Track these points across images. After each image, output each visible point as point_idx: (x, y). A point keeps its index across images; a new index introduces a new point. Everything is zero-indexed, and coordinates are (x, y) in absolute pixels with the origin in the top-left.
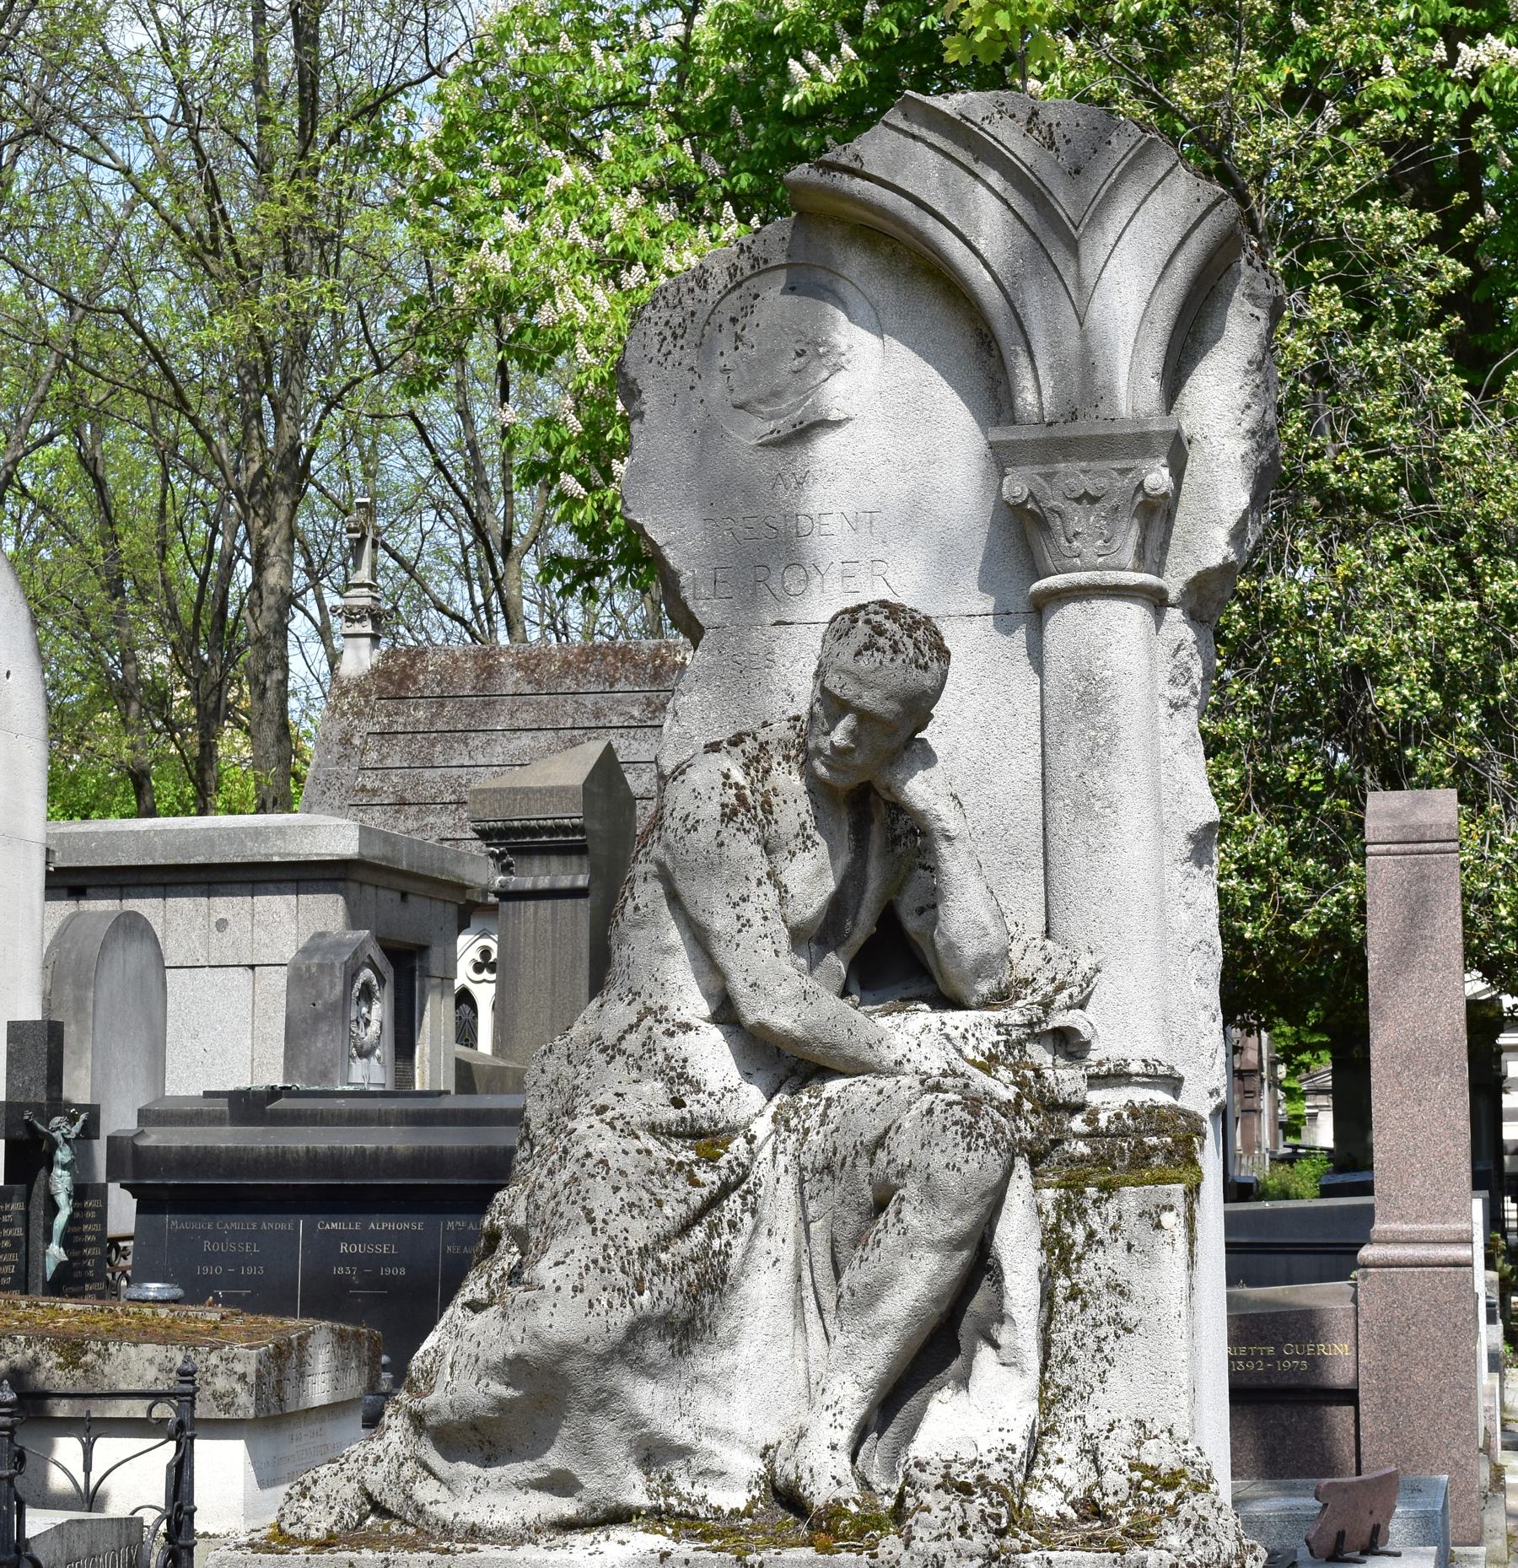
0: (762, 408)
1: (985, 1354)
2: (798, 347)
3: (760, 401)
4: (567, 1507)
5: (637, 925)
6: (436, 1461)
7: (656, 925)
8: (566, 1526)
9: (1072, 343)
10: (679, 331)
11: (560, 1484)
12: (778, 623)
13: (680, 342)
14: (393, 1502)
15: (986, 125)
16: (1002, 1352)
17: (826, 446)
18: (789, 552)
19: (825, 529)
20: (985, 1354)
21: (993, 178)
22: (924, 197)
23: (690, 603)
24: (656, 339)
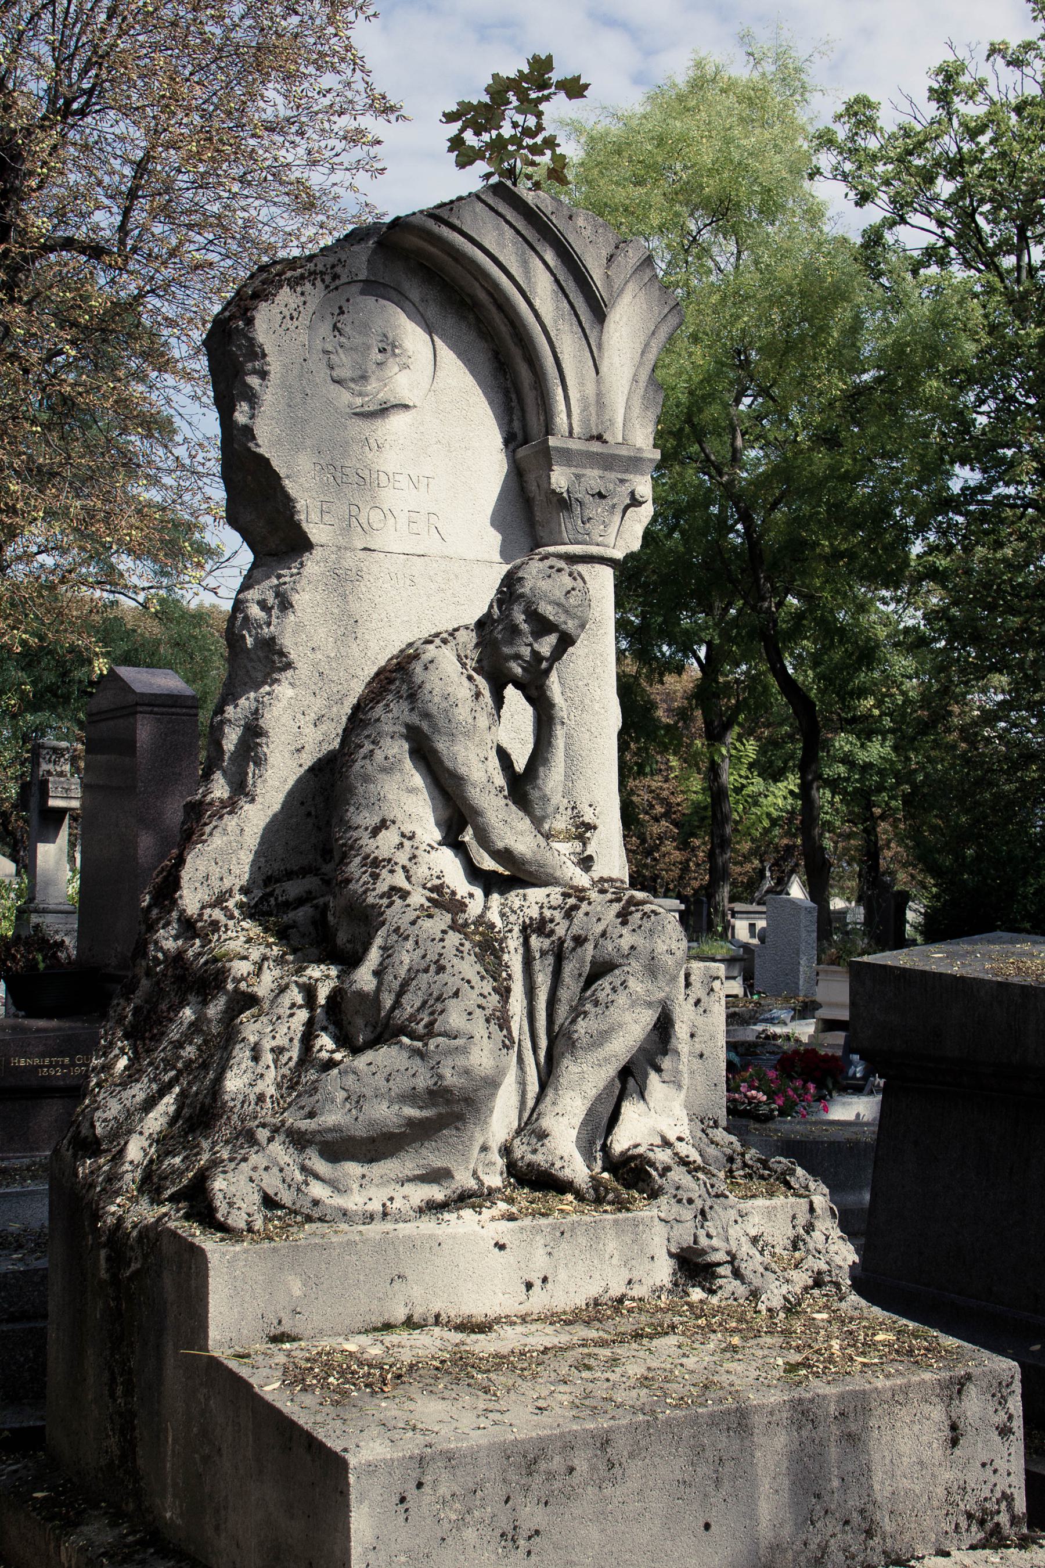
0: (352, 385)
1: (653, 1077)
2: (380, 345)
3: (353, 380)
4: (437, 1193)
5: (383, 770)
6: (321, 1166)
7: (401, 770)
8: (442, 1206)
9: (590, 389)
10: (295, 314)
11: (437, 1176)
12: (365, 549)
13: (296, 323)
14: (286, 1197)
15: (553, 218)
16: (664, 1074)
17: (397, 421)
18: (373, 498)
19: (397, 485)
20: (653, 1077)
21: (550, 256)
22: (501, 259)
23: (304, 525)
24: (280, 316)
